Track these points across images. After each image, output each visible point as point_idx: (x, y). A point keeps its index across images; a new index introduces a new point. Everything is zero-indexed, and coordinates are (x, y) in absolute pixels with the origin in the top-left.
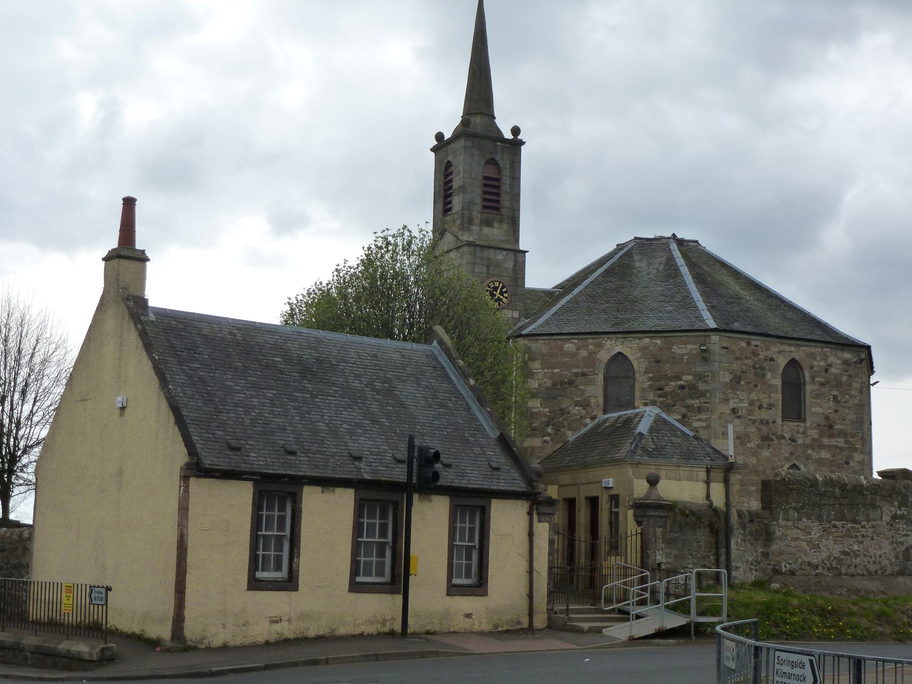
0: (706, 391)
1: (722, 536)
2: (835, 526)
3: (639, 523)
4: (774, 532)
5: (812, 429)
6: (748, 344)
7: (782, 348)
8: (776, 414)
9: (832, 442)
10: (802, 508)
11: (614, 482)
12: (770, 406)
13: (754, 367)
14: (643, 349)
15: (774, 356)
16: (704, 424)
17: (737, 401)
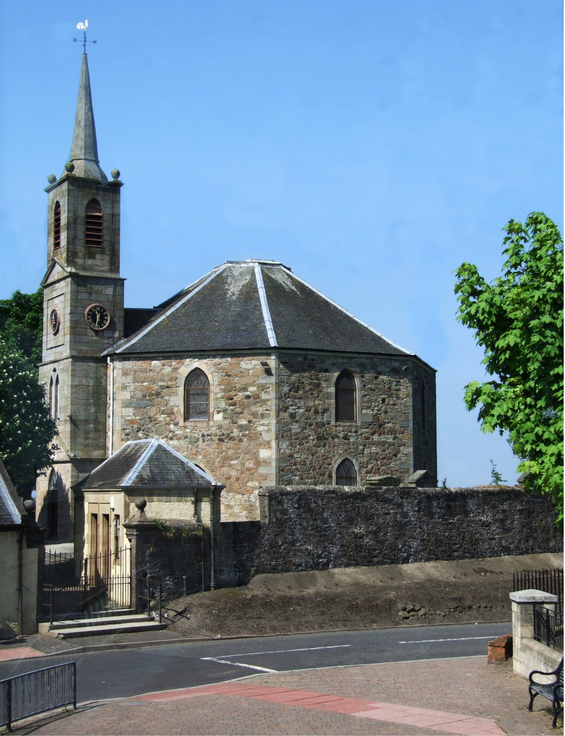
0: (268, 400)
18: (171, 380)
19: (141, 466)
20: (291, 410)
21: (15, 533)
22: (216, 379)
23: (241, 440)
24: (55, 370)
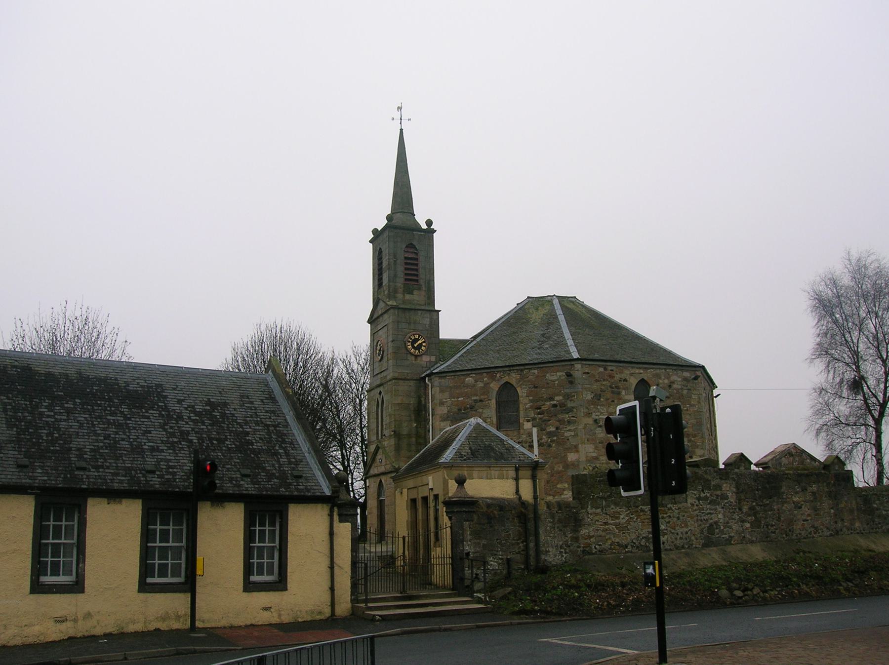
0: (573, 408)
1: (531, 525)
4: (583, 519)
6: (605, 369)
7: (633, 371)
10: (610, 496)
13: (611, 387)
15: (627, 378)
16: (573, 434)
18: (483, 394)
19: (460, 443)
20: (594, 416)
21: (325, 505)
22: (525, 391)
23: (550, 446)
24: (380, 393)
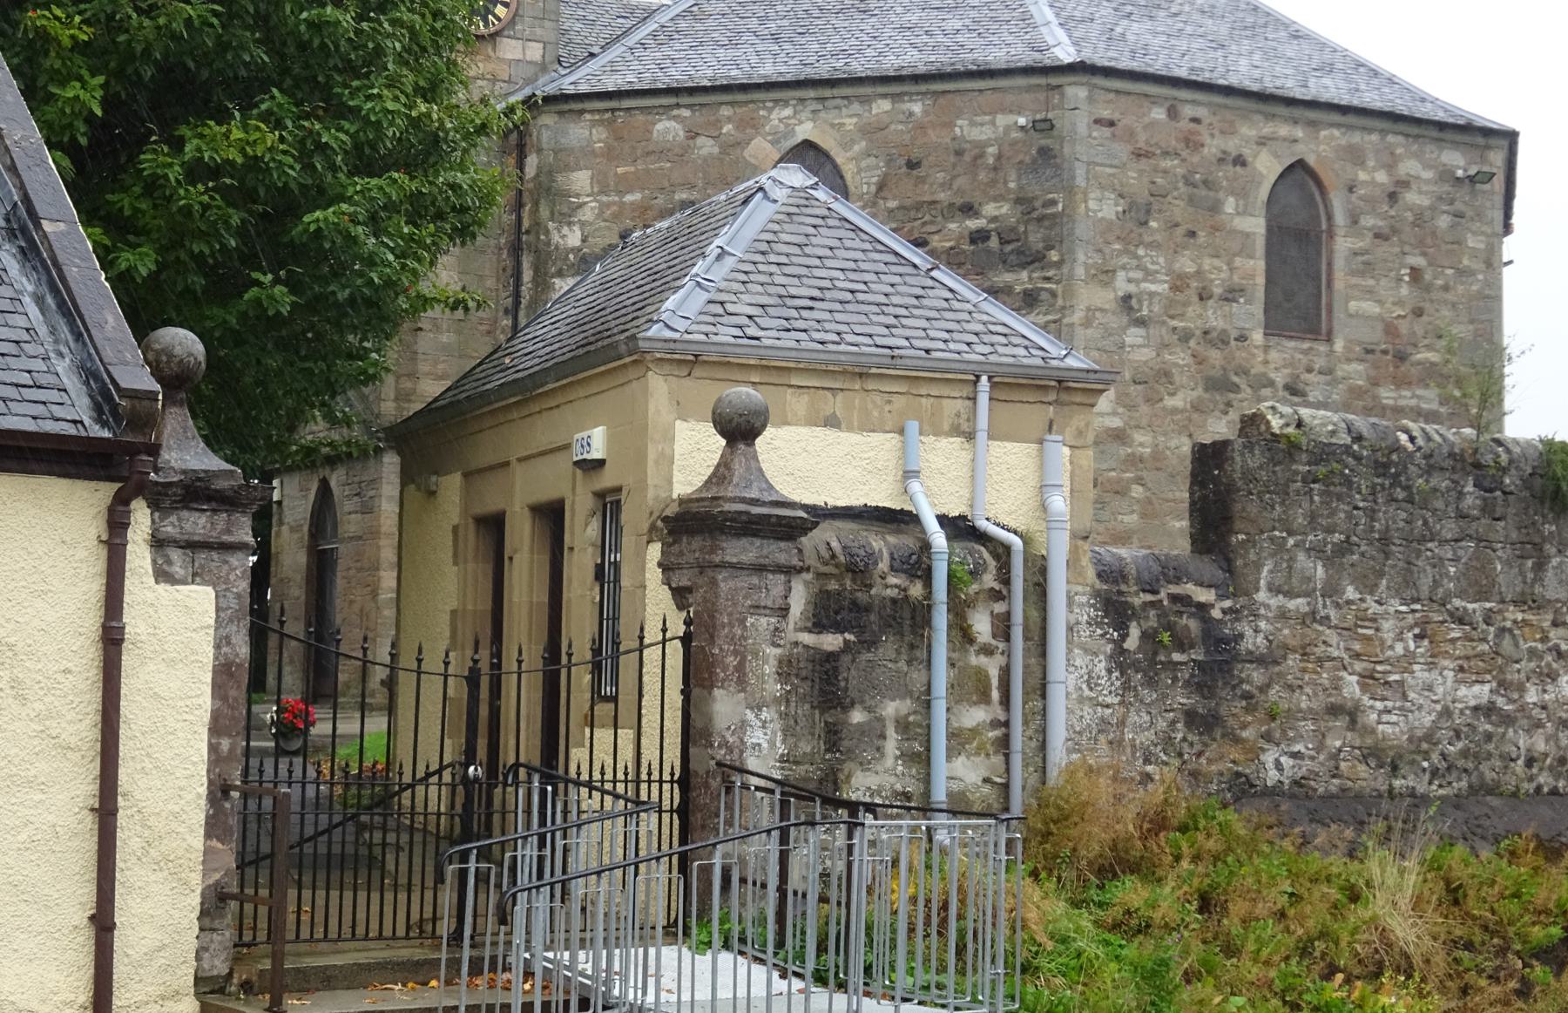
2: (1461, 619)
3: (680, 595)
5: (1349, 360)
6: (1173, 113)
7: (1267, 129)
8: (1250, 314)
9: (1407, 398)
10: (1345, 548)
11: (611, 440)
12: (1232, 294)
13: (1189, 182)
14: (871, 131)
15: (1246, 152)
17: (1138, 275)
